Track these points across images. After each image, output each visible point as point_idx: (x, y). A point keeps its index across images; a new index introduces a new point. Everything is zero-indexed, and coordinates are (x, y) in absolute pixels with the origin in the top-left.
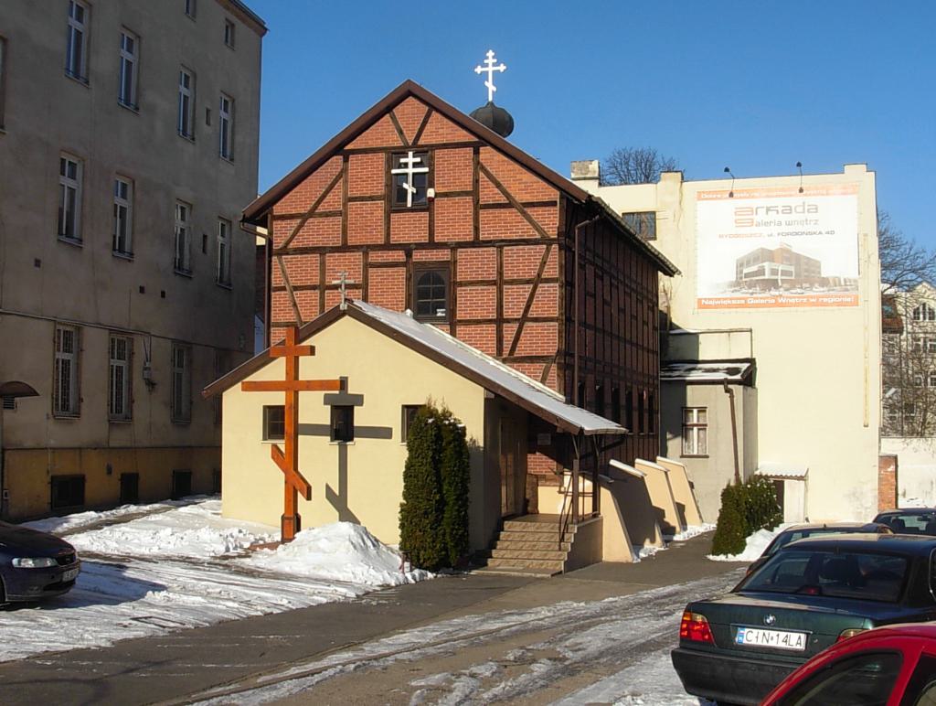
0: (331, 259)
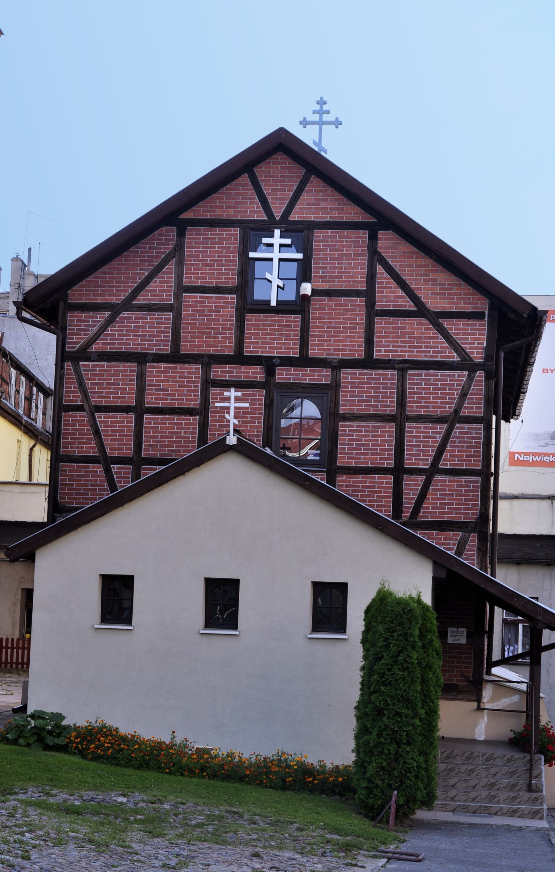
0: (154, 371)
